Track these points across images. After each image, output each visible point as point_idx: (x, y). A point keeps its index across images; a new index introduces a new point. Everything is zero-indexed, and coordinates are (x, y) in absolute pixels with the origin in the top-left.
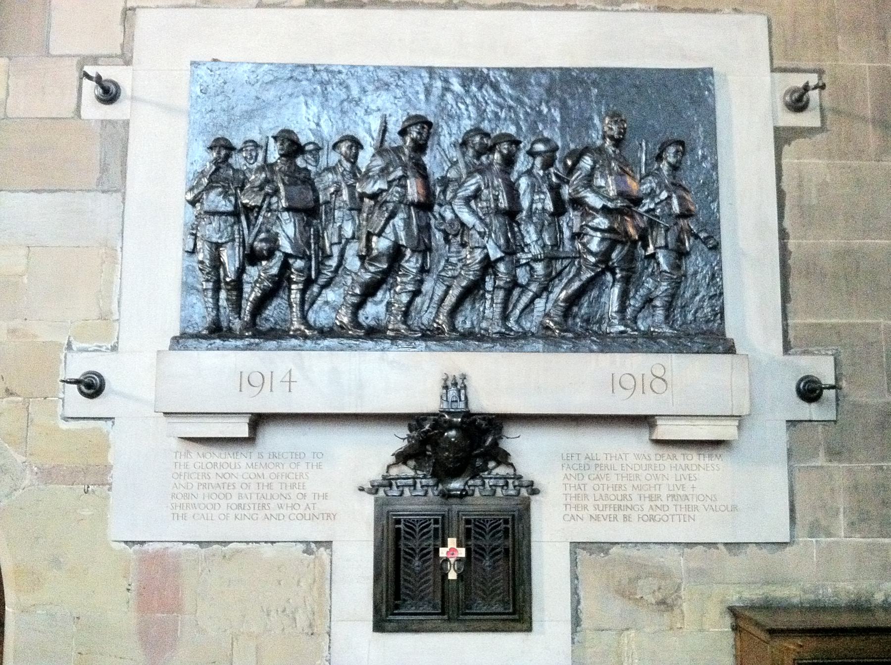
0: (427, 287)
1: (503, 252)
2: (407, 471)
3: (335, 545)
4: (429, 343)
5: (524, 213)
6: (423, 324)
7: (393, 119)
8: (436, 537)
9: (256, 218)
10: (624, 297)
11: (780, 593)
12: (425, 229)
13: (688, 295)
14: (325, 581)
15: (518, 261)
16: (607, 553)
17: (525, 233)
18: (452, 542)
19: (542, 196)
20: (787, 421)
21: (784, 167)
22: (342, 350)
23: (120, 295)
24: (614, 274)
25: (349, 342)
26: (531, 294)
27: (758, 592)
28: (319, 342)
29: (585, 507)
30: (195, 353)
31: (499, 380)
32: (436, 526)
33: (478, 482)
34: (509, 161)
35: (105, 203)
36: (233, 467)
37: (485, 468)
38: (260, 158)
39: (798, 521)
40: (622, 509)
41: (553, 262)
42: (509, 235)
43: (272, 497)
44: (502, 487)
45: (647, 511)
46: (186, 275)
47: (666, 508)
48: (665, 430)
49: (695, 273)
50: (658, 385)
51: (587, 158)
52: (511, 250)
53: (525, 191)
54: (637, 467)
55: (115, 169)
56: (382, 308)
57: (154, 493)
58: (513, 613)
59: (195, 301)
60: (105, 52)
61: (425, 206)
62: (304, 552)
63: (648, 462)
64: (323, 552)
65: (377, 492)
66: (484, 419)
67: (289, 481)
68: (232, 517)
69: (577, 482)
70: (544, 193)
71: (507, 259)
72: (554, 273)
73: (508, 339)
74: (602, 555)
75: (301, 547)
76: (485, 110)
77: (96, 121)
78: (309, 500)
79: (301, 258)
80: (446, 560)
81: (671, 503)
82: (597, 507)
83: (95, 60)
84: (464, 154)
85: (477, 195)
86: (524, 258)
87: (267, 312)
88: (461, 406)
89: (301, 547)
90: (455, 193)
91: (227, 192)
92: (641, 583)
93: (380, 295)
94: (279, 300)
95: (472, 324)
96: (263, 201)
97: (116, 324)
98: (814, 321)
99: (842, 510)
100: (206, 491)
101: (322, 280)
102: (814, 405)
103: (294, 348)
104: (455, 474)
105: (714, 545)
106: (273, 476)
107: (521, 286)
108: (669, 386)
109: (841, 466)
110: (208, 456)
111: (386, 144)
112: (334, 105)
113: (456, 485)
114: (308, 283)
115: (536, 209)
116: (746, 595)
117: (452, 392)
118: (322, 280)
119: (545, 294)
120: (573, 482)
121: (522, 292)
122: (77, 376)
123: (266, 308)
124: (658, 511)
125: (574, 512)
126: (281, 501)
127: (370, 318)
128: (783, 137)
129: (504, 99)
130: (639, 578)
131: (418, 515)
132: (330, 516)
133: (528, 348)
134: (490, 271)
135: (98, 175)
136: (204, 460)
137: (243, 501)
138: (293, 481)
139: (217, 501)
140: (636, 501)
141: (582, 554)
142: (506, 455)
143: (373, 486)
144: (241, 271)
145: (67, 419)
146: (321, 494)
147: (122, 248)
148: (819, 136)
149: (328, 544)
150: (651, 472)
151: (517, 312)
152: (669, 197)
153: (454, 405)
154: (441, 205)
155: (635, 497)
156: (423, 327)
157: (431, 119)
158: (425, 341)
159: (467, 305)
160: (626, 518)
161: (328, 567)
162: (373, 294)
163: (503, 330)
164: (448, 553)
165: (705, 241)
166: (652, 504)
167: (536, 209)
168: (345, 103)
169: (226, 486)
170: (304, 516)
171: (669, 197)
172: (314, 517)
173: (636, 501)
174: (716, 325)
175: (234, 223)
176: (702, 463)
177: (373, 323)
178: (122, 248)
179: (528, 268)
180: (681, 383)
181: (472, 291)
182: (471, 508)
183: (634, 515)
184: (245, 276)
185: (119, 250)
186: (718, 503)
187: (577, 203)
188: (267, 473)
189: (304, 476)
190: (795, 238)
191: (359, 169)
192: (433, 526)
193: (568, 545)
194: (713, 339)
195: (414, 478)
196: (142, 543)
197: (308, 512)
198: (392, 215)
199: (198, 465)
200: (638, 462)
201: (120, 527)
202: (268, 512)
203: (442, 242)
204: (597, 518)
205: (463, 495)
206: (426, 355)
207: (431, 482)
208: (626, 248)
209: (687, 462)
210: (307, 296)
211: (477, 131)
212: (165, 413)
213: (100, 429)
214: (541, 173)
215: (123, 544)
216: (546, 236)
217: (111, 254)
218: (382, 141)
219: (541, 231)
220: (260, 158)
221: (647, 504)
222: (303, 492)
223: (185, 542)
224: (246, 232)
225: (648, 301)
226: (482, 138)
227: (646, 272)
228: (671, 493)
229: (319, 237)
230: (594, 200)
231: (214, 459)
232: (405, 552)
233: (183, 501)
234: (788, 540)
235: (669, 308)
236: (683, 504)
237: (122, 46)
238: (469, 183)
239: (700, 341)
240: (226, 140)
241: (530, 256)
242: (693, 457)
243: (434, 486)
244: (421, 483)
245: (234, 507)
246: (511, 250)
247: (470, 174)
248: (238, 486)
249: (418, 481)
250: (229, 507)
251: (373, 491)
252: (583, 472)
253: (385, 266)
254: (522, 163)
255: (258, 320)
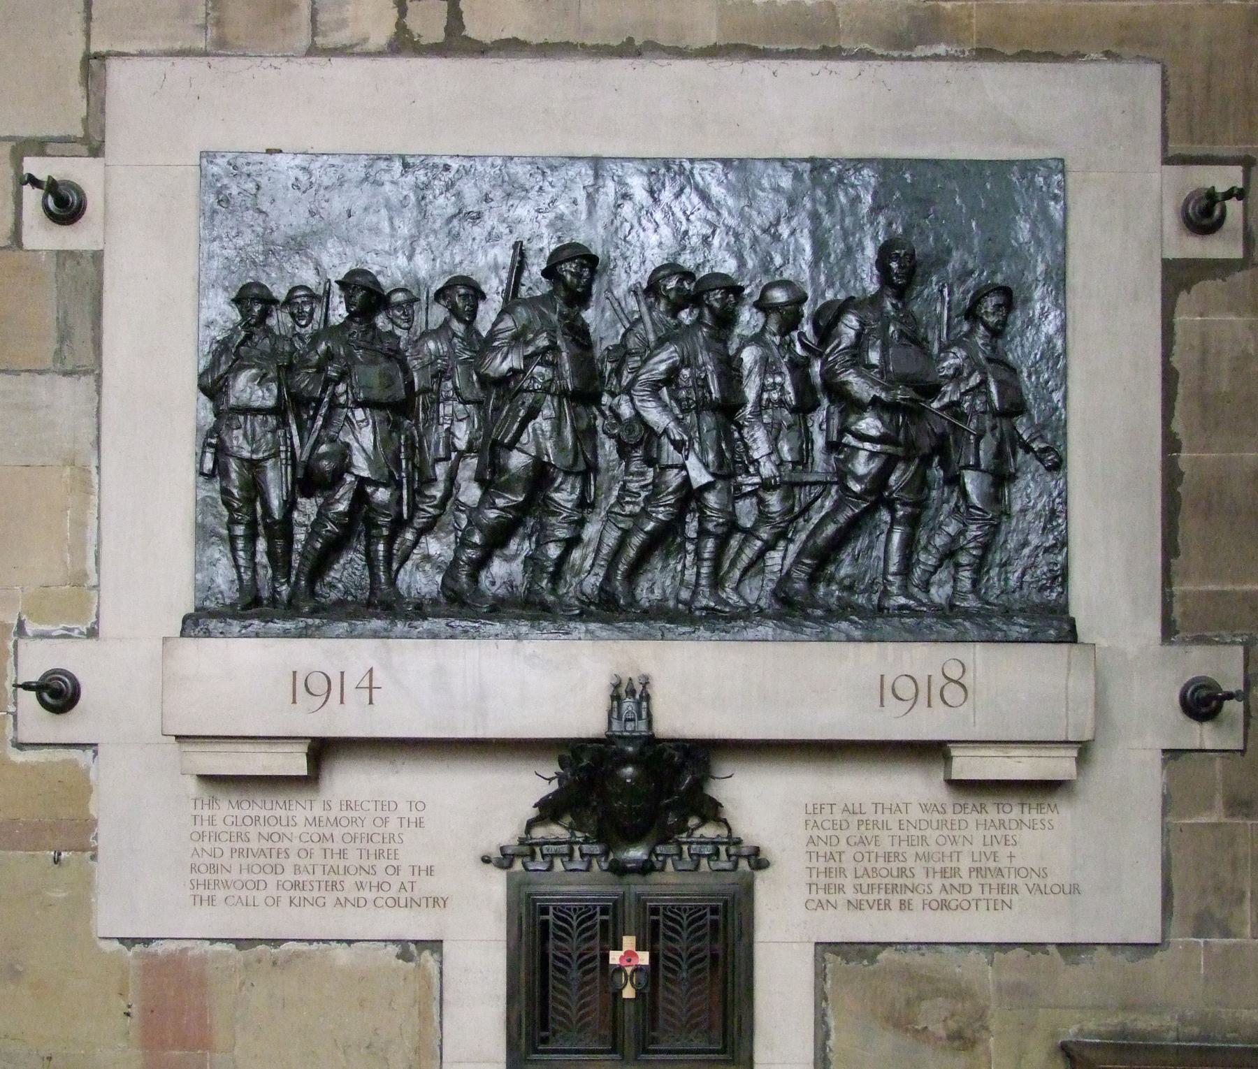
0: (590, 531)
1: (713, 474)
2: (557, 831)
3: (446, 947)
4: (592, 626)
5: (749, 408)
6: (584, 594)
7: (536, 245)
8: (604, 937)
9: (314, 419)
10: (909, 546)
11: (1145, 1023)
12: (586, 436)
13: (1011, 545)
14: (432, 1003)
15: (738, 487)
16: (873, 959)
17: (750, 443)
18: (629, 942)
19: (778, 379)
20: (1164, 751)
21: (1178, 330)
22: (452, 637)
23: (99, 544)
24: (893, 511)
25: (464, 623)
26: (759, 543)
27: (1108, 1021)
28: (416, 623)
29: (840, 888)
30: (221, 642)
31: (703, 684)
32: (605, 917)
33: (672, 849)
34: (725, 320)
35: (67, 394)
36: (284, 822)
37: (683, 828)
38: (318, 315)
39: (1176, 910)
40: (895, 891)
41: (796, 490)
42: (724, 446)
43: (346, 870)
44: (709, 857)
45: (937, 894)
46: (203, 513)
47: (967, 890)
48: (967, 765)
49: (1024, 511)
50: (953, 693)
51: (851, 317)
52: (730, 467)
53: (750, 372)
54: (924, 825)
55: (82, 332)
56: (517, 566)
57: (157, 874)
58: (723, 1051)
59: (217, 556)
60: (55, 133)
61: (585, 396)
62: (398, 957)
63: (940, 817)
64: (428, 958)
65: (510, 865)
66: (677, 748)
67: (372, 847)
68: (285, 901)
69: (828, 849)
70: (781, 374)
71: (719, 486)
72: (797, 509)
73: (719, 619)
74: (865, 962)
75: (393, 949)
76: (686, 232)
77: (49, 252)
78: (405, 876)
79: (386, 486)
80: (619, 969)
81: (975, 882)
82: (858, 889)
83: (40, 147)
84: (650, 308)
85: (671, 377)
86: (749, 482)
87: (332, 574)
88: (642, 726)
89: (393, 949)
90: (636, 371)
91: (265, 375)
92: (925, 1005)
93: (513, 545)
94: (351, 555)
95: (664, 592)
96: (324, 391)
97: (94, 592)
98: (1212, 587)
99: (1249, 894)
100: (244, 861)
101: (419, 522)
102: (1207, 726)
103: (375, 635)
104: (633, 838)
105: (1041, 946)
106: (348, 839)
107: (744, 530)
108: (970, 694)
109: (1249, 822)
110: (245, 805)
111: (523, 292)
112: (437, 225)
113: (637, 853)
114: (399, 525)
115: (769, 400)
116: (1091, 1025)
117: (628, 705)
118: (419, 522)
119: (782, 544)
120: (823, 849)
121: (745, 541)
122: (34, 678)
123: (330, 568)
124: (955, 895)
125: (822, 896)
126: (363, 877)
127: (498, 584)
128: (1178, 277)
129: (719, 214)
130: (921, 998)
131: (574, 900)
132: (438, 902)
133: (750, 633)
134: (693, 505)
135: (56, 346)
136: (236, 812)
137: (301, 878)
138: (378, 846)
139: (261, 876)
140: (920, 878)
141: (832, 959)
142: (716, 805)
143: (504, 855)
144: (290, 505)
145: (20, 746)
146: (423, 867)
147: (98, 468)
148: (1239, 276)
149: (435, 946)
150: (945, 832)
151: (737, 574)
152: (984, 382)
153: (630, 726)
154: (613, 395)
155: (919, 872)
156: (584, 598)
157: (597, 250)
158: (584, 622)
159: (657, 562)
160: (905, 906)
161: (436, 981)
162: (504, 544)
163: (712, 604)
164: (621, 958)
165: (1040, 456)
166: (947, 882)
167: (769, 400)
168: (455, 222)
169: (274, 853)
170: (397, 902)
171: (984, 382)
172: (412, 903)
173: (920, 878)
174: (1054, 595)
175: (278, 427)
176: (1026, 817)
177: (502, 592)
178: (98, 468)
179: (754, 500)
180: (998, 690)
181: (664, 539)
182: (657, 889)
183: (917, 900)
184: (295, 515)
185: (94, 471)
186: (1050, 881)
187: (838, 393)
188: (338, 832)
189: (396, 838)
190: (1191, 450)
191: (479, 334)
192: (599, 918)
193: (811, 948)
194: (1051, 621)
195: (570, 843)
196: (147, 941)
197: (403, 895)
198: (533, 413)
199: (229, 820)
200: (926, 816)
201: (113, 917)
202: (341, 895)
203: (615, 456)
204: (858, 906)
205: (645, 868)
206: (586, 646)
207: (597, 849)
208: (913, 468)
209: (1002, 816)
210: (396, 546)
211: (672, 268)
212: (177, 737)
213: (75, 763)
214: (777, 340)
215: (117, 944)
216: (785, 448)
217: (84, 480)
218: (517, 284)
219: (776, 439)
220: (318, 315)
221: (937, 883)
222: (395, 863)
223: (213, 941)
224: (296, 440)
225: (949, 555)
226: (680, 281)
227: (946, 508)
228: (977, 865)
229: (414, 447)
230: (858, 386)
231: (255, 811)
232: (555, 957)
233: (208, 876)
234: (1158, 941)
235: (980, 567)
236: (994, 882)
237: (85, 121)
238: (656, 359)
239: (1022, 621)
240: (264, 287)
241: (757, 480)
242: (1014, 811)
243: (601, 855)
244: (580, 850)
245: (288, 885)
246: (730, 467)
247: (661, 342)
248: (293, 854)
249: (576, 848)
250: (279, 885)
251: (506, 863)
252: (838, 833)
253: (521, 499)
254: (748, 319)
255: (317, 588)
